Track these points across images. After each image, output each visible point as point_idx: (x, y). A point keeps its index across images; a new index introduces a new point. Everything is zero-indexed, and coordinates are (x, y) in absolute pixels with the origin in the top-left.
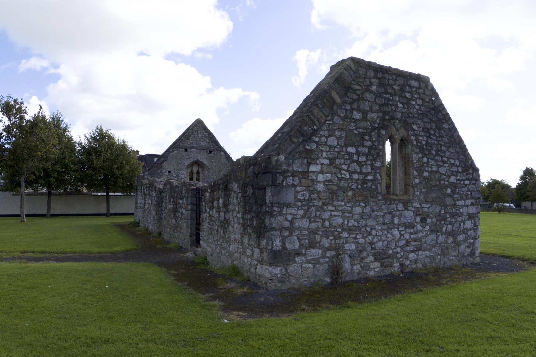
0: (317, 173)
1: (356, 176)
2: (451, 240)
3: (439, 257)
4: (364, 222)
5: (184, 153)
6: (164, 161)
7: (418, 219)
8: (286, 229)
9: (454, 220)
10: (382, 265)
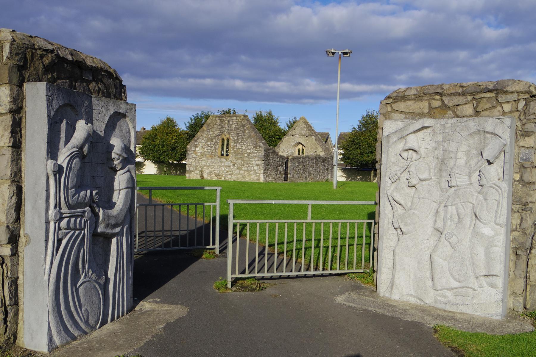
7: (231, 164)
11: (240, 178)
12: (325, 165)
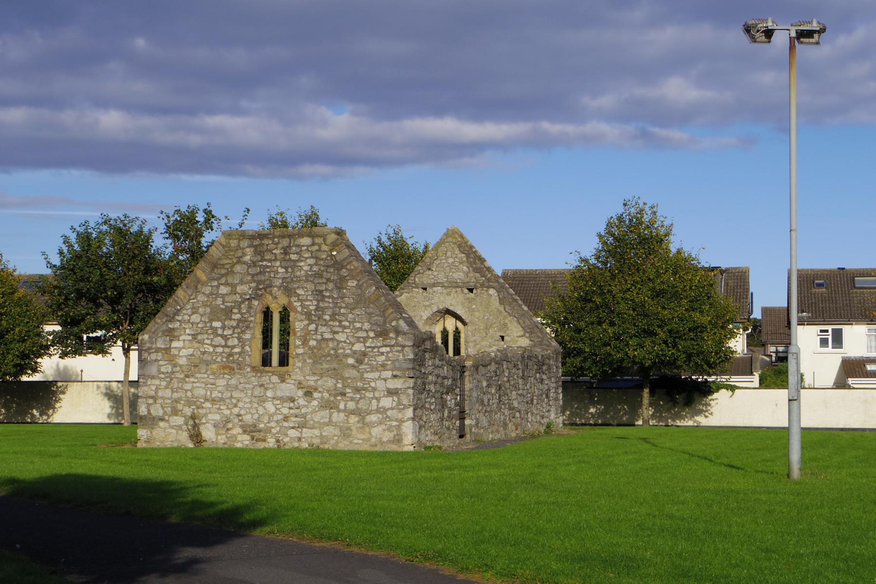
0: (180, 349)
1: (220, 350)
3: (336, 438)
4: (229, 395)
7: (300, 393)
8: (151, 397)
10: (253, 439)
11: (335, 442)
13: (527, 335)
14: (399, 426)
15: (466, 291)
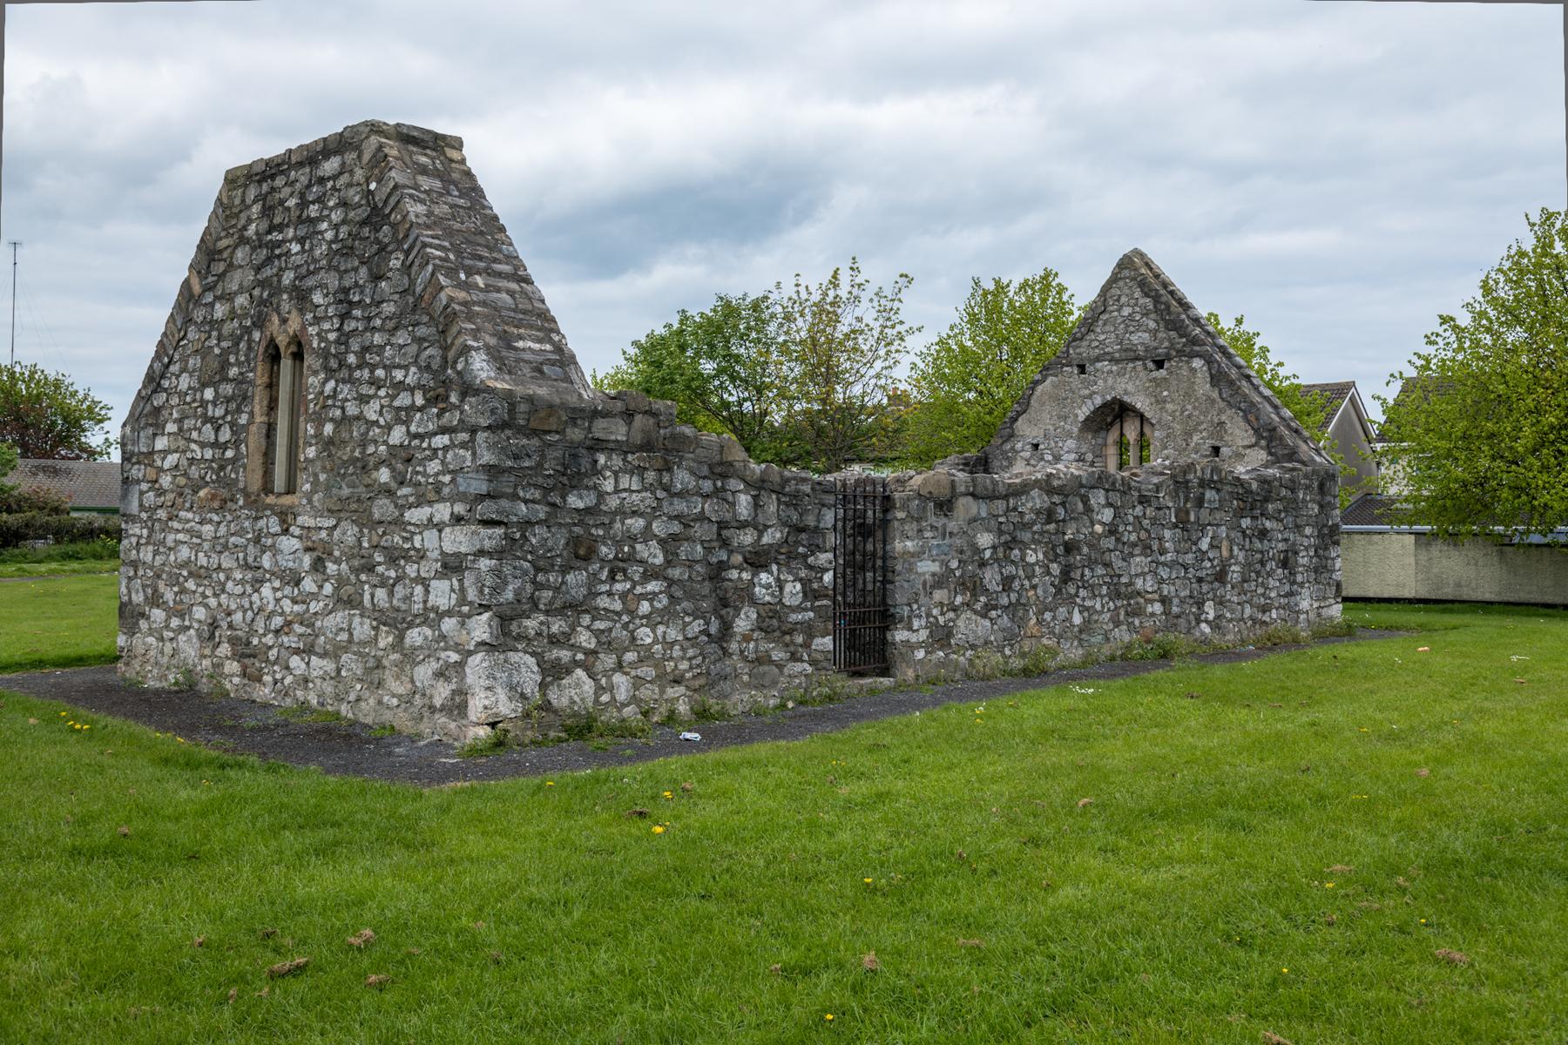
0: (165, 453)
1: (209, 454)
2: (386, 640)
3: (358, 687)
5: (1075, 380)
6: (1019, 414)
7: (307, 560)
9: (393, 574)
12: (1263, 534)
13: (1263, 443)
14: (461, 665)
15: (1151, 365)
